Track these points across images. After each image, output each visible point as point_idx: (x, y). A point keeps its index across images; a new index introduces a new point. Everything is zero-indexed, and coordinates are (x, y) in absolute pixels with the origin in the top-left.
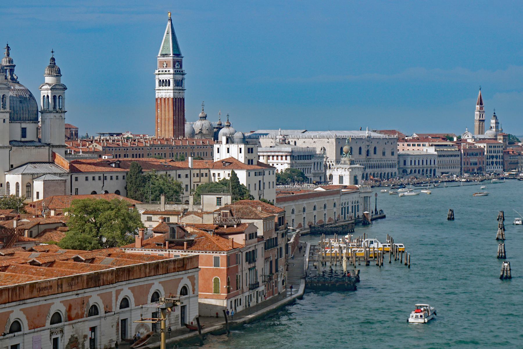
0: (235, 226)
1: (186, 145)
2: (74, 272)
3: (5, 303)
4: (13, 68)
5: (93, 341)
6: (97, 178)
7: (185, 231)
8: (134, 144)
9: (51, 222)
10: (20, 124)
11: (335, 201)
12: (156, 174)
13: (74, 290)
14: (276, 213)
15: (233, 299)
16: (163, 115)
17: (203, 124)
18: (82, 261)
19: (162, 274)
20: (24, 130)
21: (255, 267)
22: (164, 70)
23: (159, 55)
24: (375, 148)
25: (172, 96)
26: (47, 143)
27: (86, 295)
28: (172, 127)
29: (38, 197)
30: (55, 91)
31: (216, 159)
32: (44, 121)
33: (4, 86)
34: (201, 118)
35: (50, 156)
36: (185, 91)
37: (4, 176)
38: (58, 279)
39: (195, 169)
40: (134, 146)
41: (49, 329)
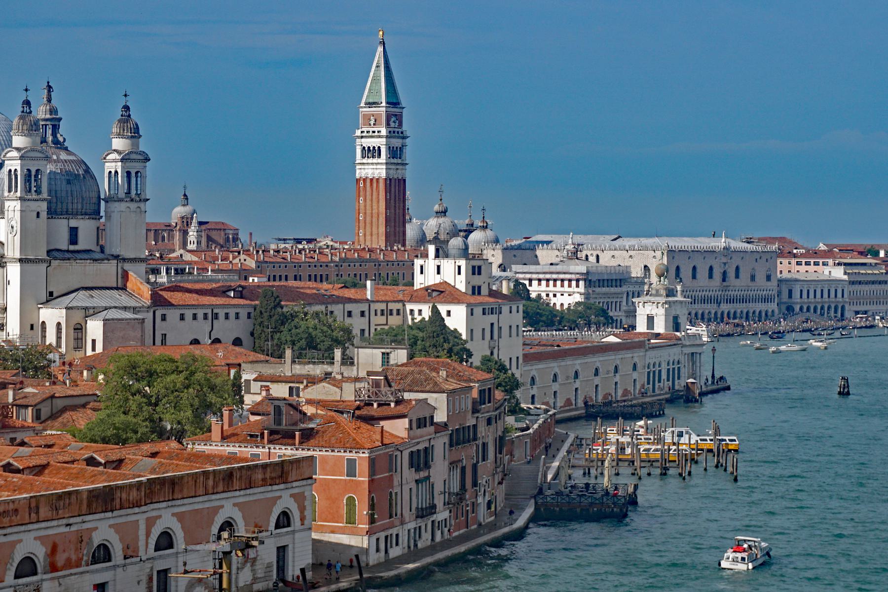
0: (393, 405)
1: (403, 259)
2: (68, 485)
4: (57, 123)
6: (200, 316)
7: (301, 412)
8: (312, 258)
9: (75, 393)
10: (65, 222)
11: (636, 360)
12: (305, 310)
14: (475, 382)
15: (382, 535)
16: (368, 207)
17: (440, 224)
18: (99, 464)
19: (240, 490)
21: (428, 477)
22: (371, 130)
23: (362, 105)
26: (115, 254)
28: (384, 230)
29: (94, 349)
30: (128, 164)
31: (418, 284)
32: (110, 216)
34: (437, 213)
35: (120, 276)
36: (407, 166)
37: (37, 310)
38: (31, 497)
39: (378, 301)
40: (311, 260)
41: (11, 587)
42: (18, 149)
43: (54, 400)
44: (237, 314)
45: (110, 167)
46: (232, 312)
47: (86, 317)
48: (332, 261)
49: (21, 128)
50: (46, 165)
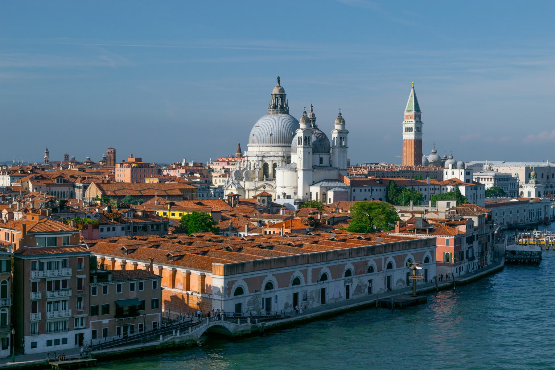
0: (460, 220)
2: (358, 245)
5: (370, 289)
6: (367, 190)
7: (427, 222)
11: (525, 208)
14: (486, 213)
15: (458, 266)
16: (408, 150)
21: (472, 247)
23: (405, 111)
24: (553, 174)
25: (414, 139)
27: (367, 259)
29: (330, 202)
30: (341, 134)
33: (310, 131)
34: (433, 153)
35: (338, 175)
42: (302, 129)
44: (380, 189)
48: (396, 171)
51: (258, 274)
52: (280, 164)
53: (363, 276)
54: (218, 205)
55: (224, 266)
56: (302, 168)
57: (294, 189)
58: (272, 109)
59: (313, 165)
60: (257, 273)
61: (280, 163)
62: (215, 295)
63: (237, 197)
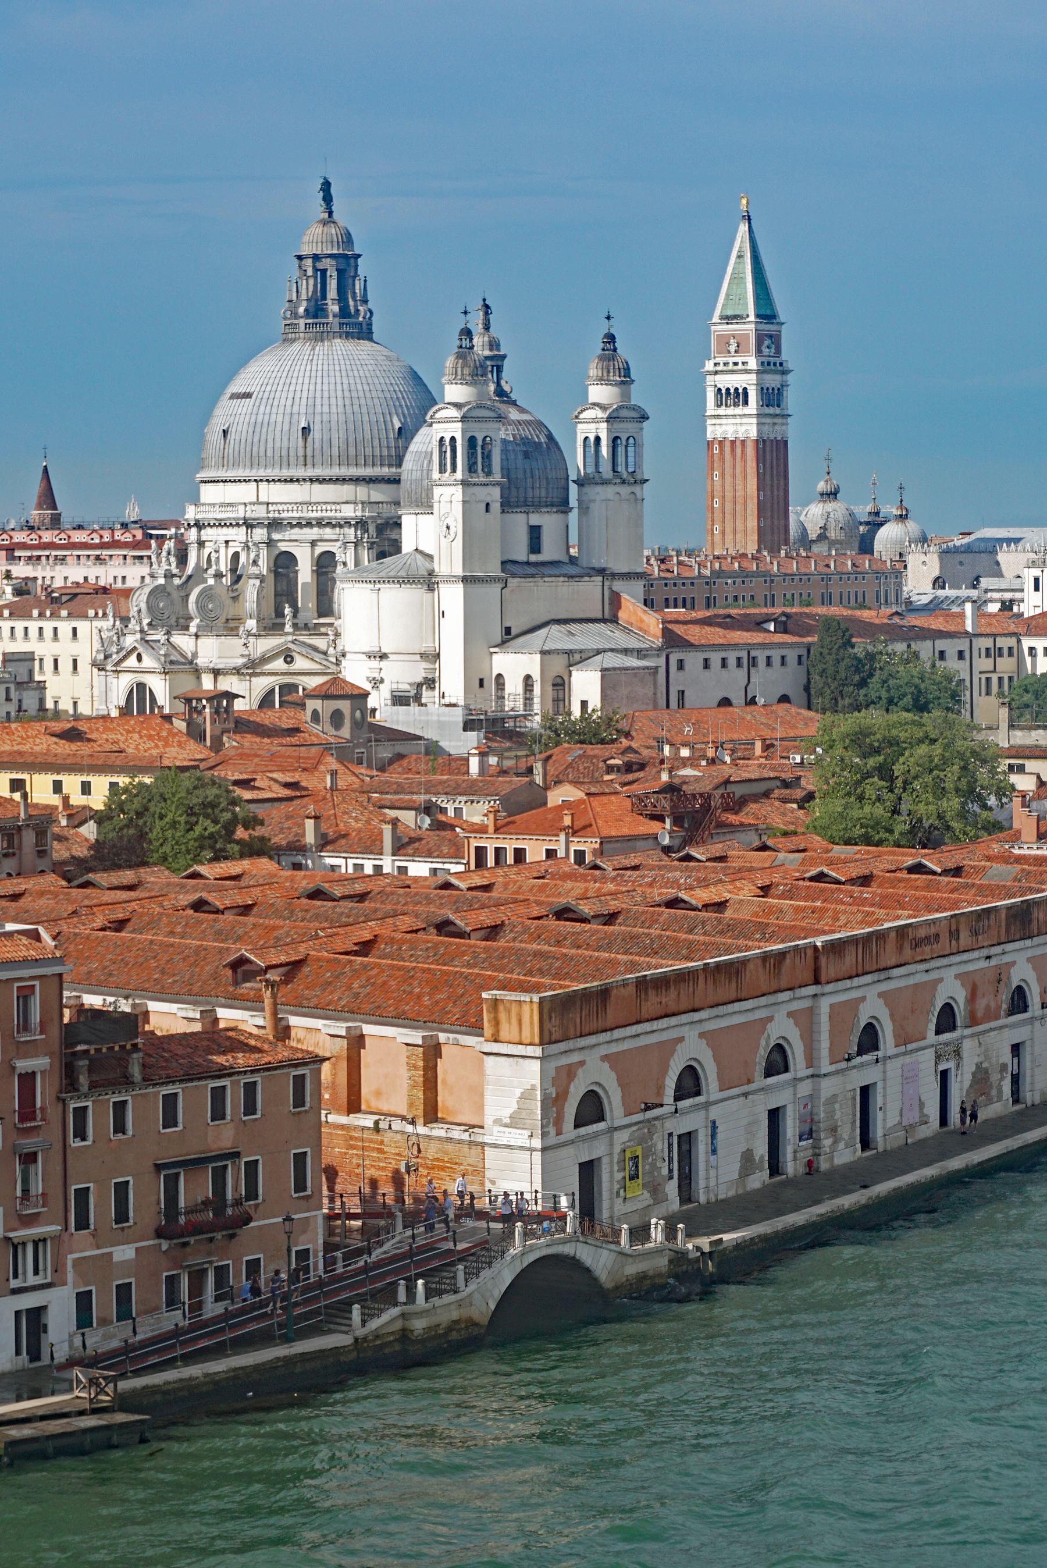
3: (850, 978)
4: (500, 363)
5: (1016, 1079)
6: (732, 662)
8: (668, 571)
9: (753, 777)
10: (524, 516)
12: (890, 648)
13: (981, 945)
16: (728, 487)
17: (829, 513)
20: (535, 532)
22: (731, 360)
23: (716, 319)
25: (753, 434)
26: (597, 566)
27: (1007, 959)
30: (616, 426)
31: (1032, 608)
32: (588, 508)
34: (822, 494)
36: (790, 419)
37: (488, 657)
39: (981, 635)
40: (668, 575)
42: (457, 406)
43: (728, 786)
45: (585, 430)
46: (776, 655)
47: (571, 665)
48: (700, 576)
49: (459, 372)
50: (499, 429)
51: (653, 1032)
52: (350, 557)
53: (991, 1030)
54: (150, 737)
55: (542, 1000)
56: (459, 571)
57: (424, 665)
58: (302, 322)
59: (505, 558)
60: (649, 1029)
61: (351, 550)
62: (497, 1128)
63: (225, 703)
